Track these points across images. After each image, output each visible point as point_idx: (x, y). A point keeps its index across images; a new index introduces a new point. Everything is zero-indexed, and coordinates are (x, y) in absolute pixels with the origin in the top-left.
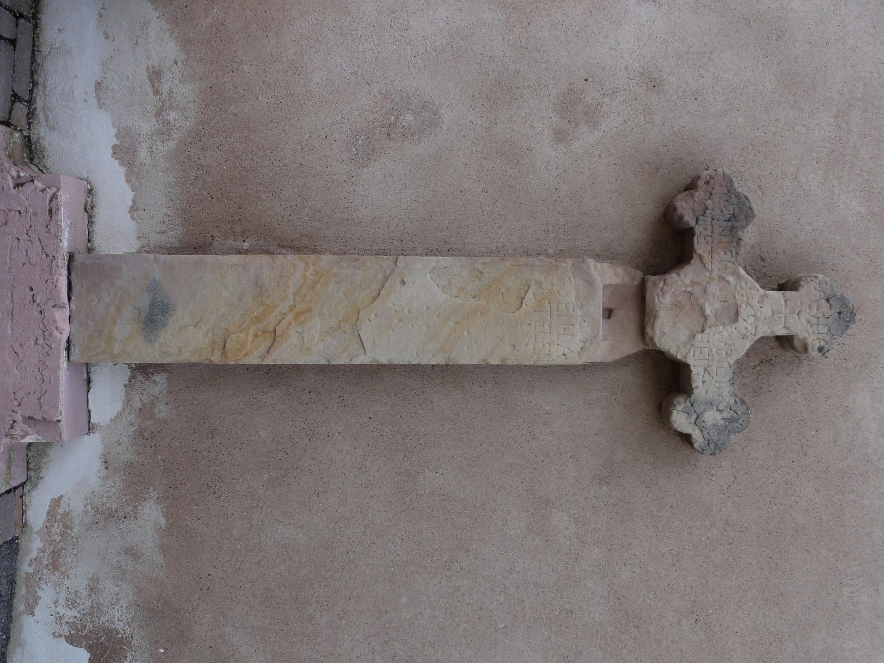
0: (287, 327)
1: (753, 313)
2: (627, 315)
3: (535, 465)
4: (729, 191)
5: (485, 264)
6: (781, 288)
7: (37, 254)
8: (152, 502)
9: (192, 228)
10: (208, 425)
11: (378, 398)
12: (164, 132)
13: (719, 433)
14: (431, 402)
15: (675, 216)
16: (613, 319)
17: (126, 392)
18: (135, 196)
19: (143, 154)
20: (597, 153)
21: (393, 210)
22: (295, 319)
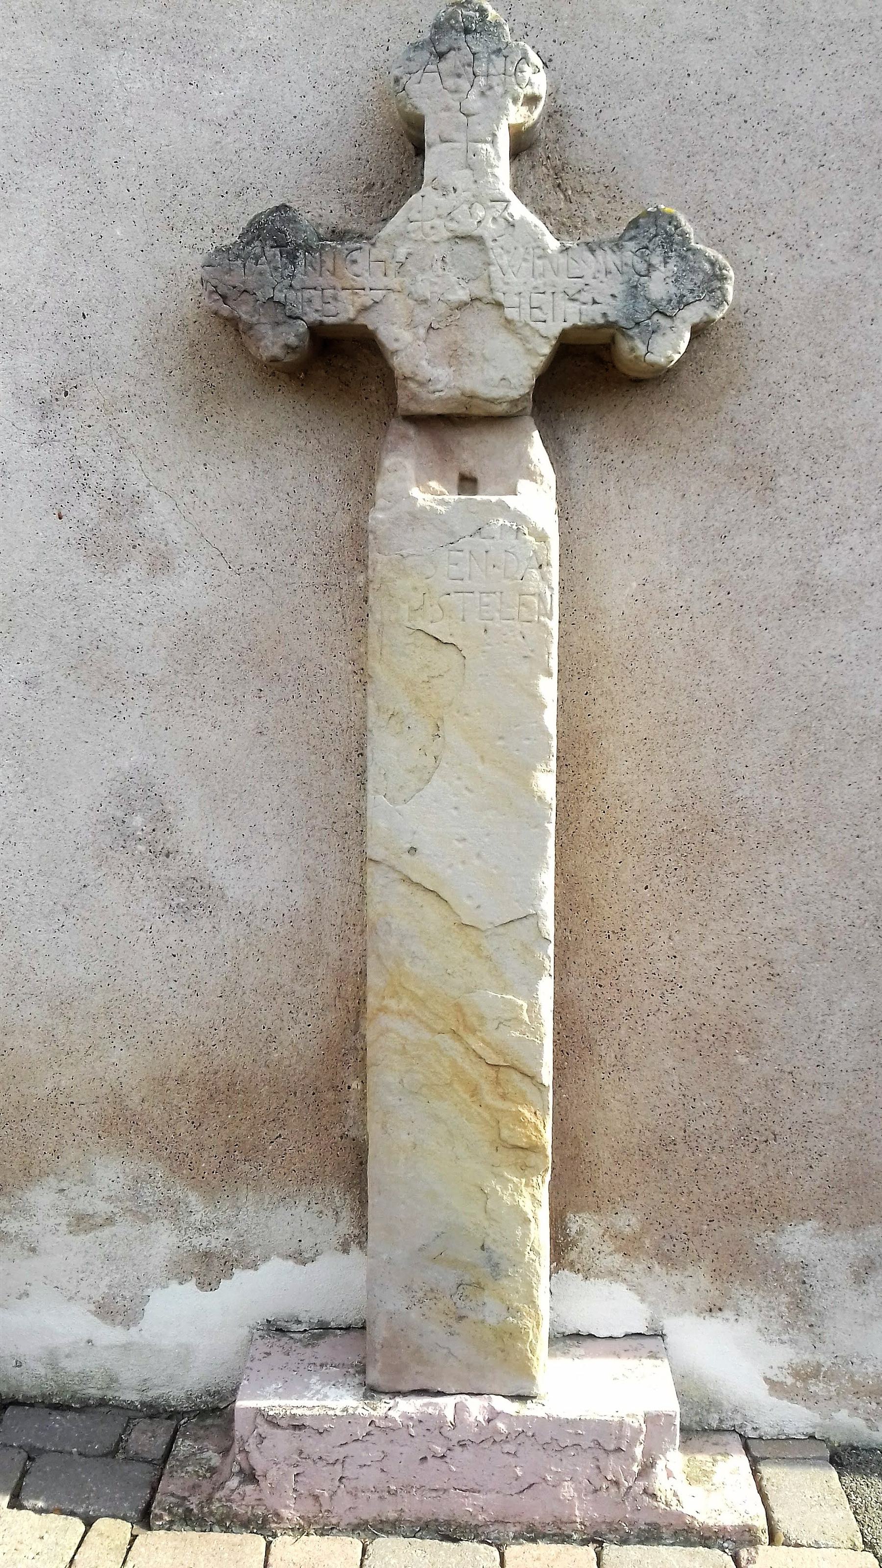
0: (488, 1044)
1: (465, 207)
2: (475, 450)
3: (735, 606)
4: (238, 256)
5: (378, 709)
6: (420, 150)
7: (367, 1450)
8: (780, 1241)
9: (328, 1169)
10: (652, 1150)
11: (611, 875)
12: (174, 1210)
13: (693, 270)
14: (620, 785)
15: (289, 359)
16: (478, 475)
17: (597, 1276)
18: (278, 1255)
19: (213, 1242)
20: (188, 498)
21: (294, 846)
22: (474, 1031)
